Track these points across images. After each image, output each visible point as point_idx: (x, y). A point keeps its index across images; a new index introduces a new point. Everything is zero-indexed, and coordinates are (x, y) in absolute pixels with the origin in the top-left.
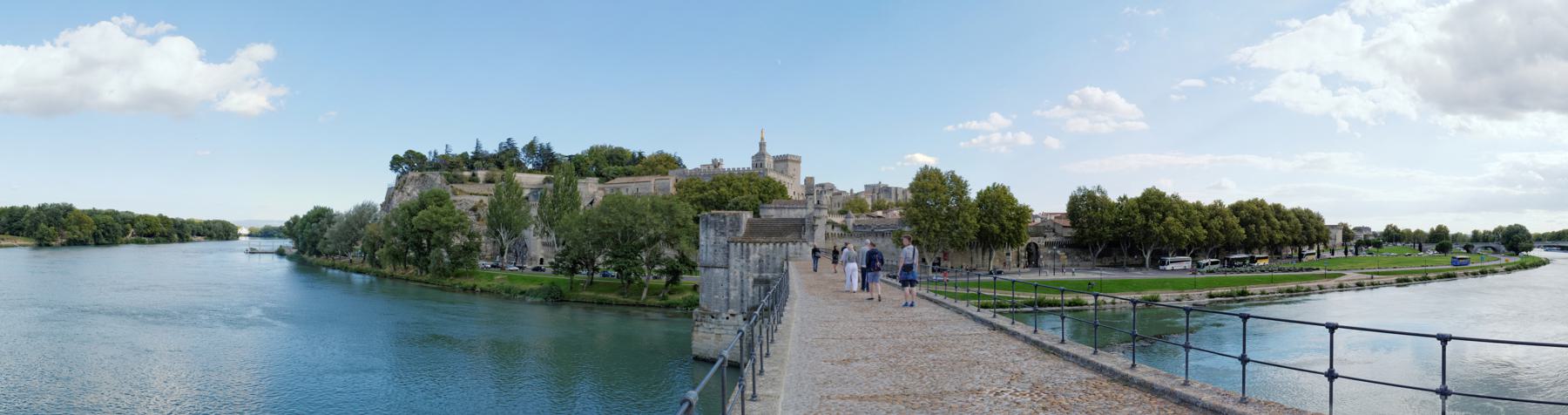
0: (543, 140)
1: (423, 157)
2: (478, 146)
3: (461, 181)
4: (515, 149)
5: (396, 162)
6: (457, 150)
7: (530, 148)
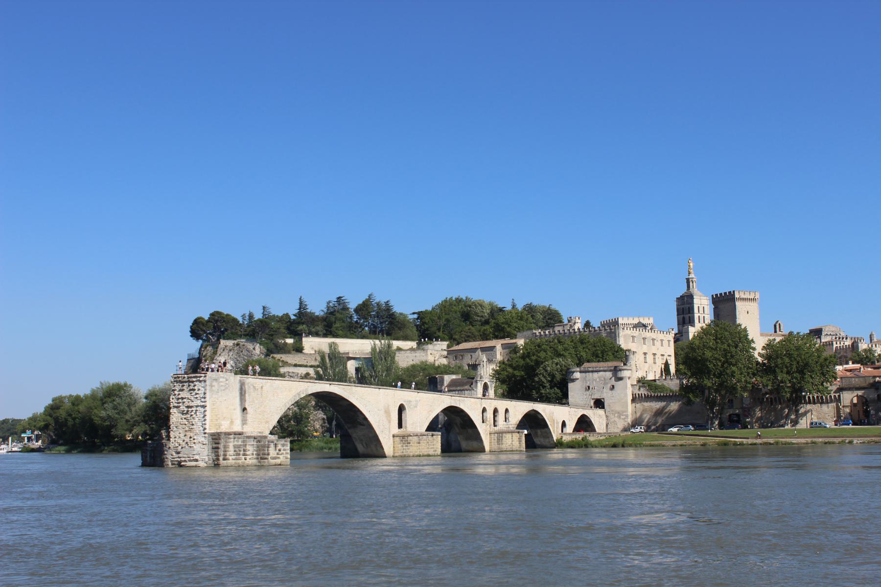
0: (380, 298)
1: (235, 320)
3: (284, 349)
4: (345, 309)
5: (198, 329)
6: (277, 311)
7: (364, 308)
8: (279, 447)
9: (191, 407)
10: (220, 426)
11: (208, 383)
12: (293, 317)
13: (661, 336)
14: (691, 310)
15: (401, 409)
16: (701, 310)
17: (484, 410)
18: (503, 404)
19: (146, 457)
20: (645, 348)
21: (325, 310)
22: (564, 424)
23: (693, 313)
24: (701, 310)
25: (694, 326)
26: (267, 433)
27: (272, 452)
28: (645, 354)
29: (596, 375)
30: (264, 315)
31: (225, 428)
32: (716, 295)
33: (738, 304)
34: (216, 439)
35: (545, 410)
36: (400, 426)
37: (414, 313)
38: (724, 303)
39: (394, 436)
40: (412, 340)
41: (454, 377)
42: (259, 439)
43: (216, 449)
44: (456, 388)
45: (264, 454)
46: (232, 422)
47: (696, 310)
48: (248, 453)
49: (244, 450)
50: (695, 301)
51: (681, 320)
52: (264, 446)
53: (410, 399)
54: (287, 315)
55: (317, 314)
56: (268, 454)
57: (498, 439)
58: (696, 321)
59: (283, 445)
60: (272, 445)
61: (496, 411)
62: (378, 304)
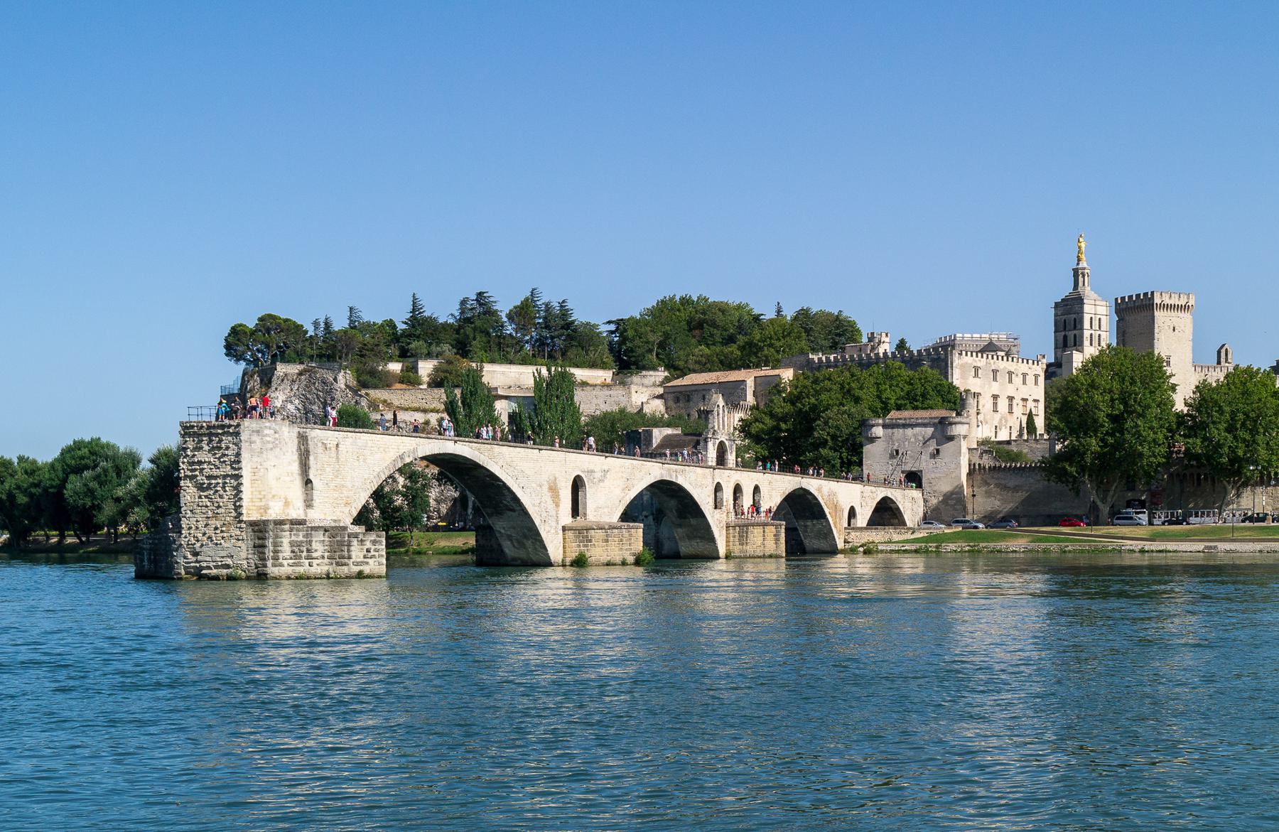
0: (550, 296)
2: (415, 308)
3: (385, 381)
6: (373, 315)
7: (523, 312)
8: (368, 545)
9: (216, 477)
10: (266, 509)
11: (244, 437)
12: (401, 327)
13: (1023, 368)
14: (1078, 324)
15: (577, 485)
16: (1096, 323)
17: (718, 488)
18: (749, 479)
19: (142, 561)
20: (995, 388)
21: (457, 314)
22: (852, 513)
23: (1082, 329)
24: (1096, 323)
25: (1082, 351)
26: (347, 520)
27: (357, 553)
28: (995, 397)
29: (909, 431)
30: (352, 322)
31: (275, 512)
32: (1123, 298)
33: (1157, 313)
34: (260, 529)
35: (820, 487)
36: (575, 512)
37: (609, 322)
38: (1135, 314)
39: (564, 529)
40: (604, 366)
41: (669, 431)
42: (334, 532)
43: (259, 548)
44: (670, 450)
45: (343, 557)
46: (287, 503)
47: (1086, 324)
48: (314, 555)
49: (308, 551)
50: (1087, 308)
51: (1061, 339)
52: (341, 543)
53: (591, 467)
54: (391, 324)
55: (441, 321)
56: (350, 558)
57: (741, 537)
58: (1086, 343)
59: (374, 542)
60: (355, 542)
61: (738, 490)
62: (547, 305)
